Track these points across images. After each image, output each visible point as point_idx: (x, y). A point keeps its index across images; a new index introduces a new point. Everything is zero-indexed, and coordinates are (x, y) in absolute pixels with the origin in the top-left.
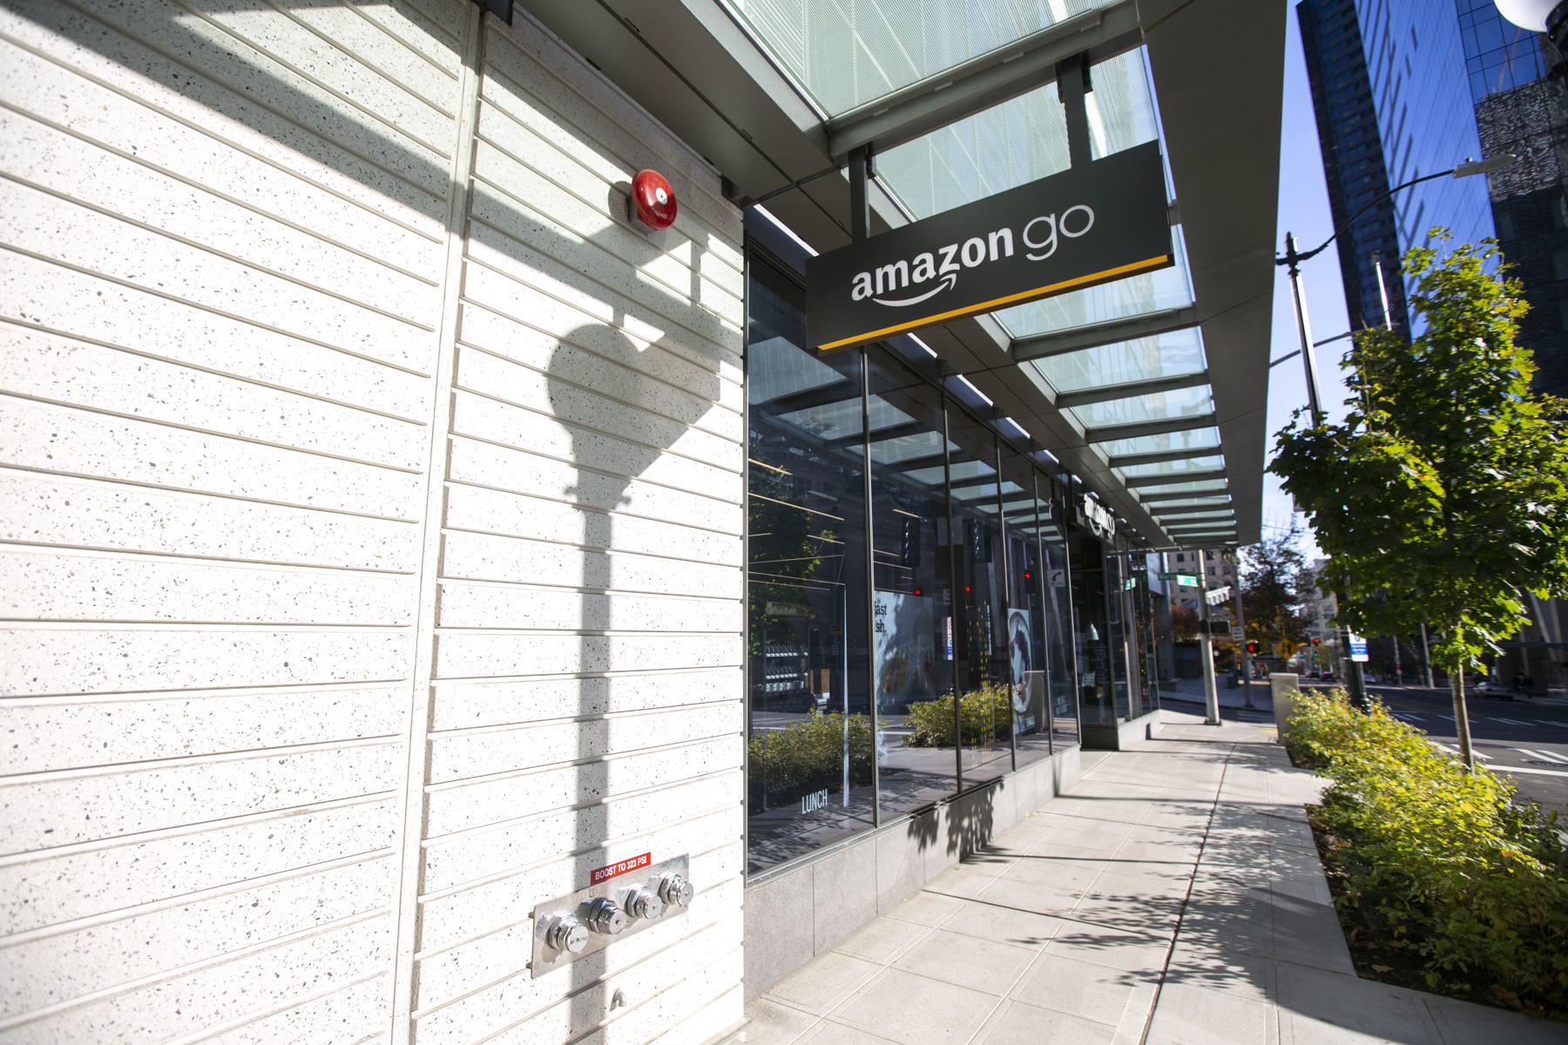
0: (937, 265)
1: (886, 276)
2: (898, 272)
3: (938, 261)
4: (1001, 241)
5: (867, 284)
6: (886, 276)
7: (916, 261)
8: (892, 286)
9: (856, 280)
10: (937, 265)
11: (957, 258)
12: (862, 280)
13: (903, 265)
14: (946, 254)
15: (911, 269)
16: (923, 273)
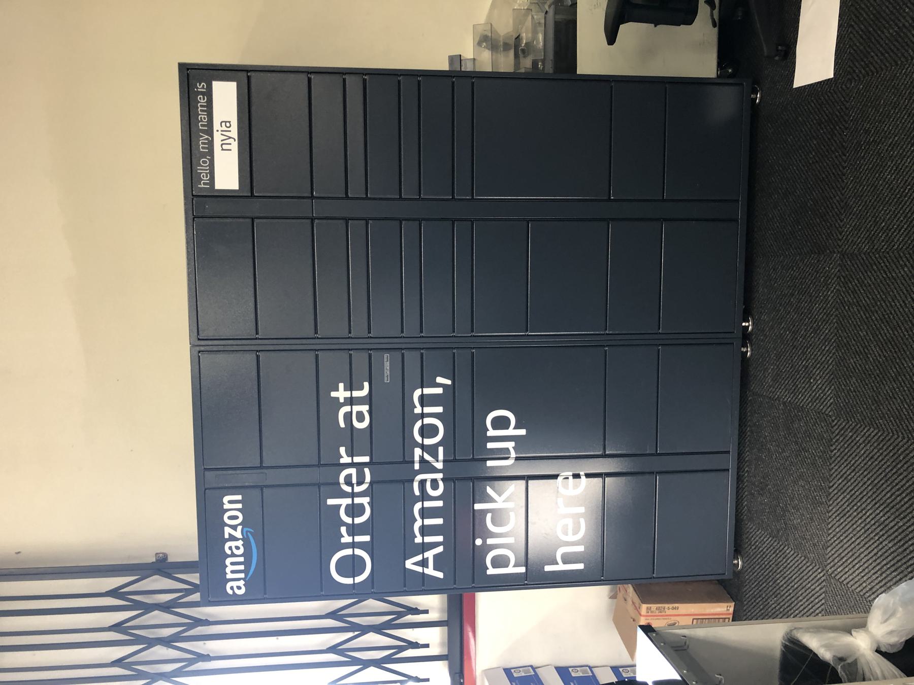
0: (236, 539)
1: (233, 572)
2: (232, 564)
3: (232, 538)
4: (230, 502)
5: (235, 584)
6: (233, 572)
7: (229, 552)
8: (242, 567)
9: (230, 592)
10: (236, 539)
11: (234, 528)
12: (232, 588)
13: (228, 561)
14: (229, 534)
15: (233, 555)
16: (237, 548)
